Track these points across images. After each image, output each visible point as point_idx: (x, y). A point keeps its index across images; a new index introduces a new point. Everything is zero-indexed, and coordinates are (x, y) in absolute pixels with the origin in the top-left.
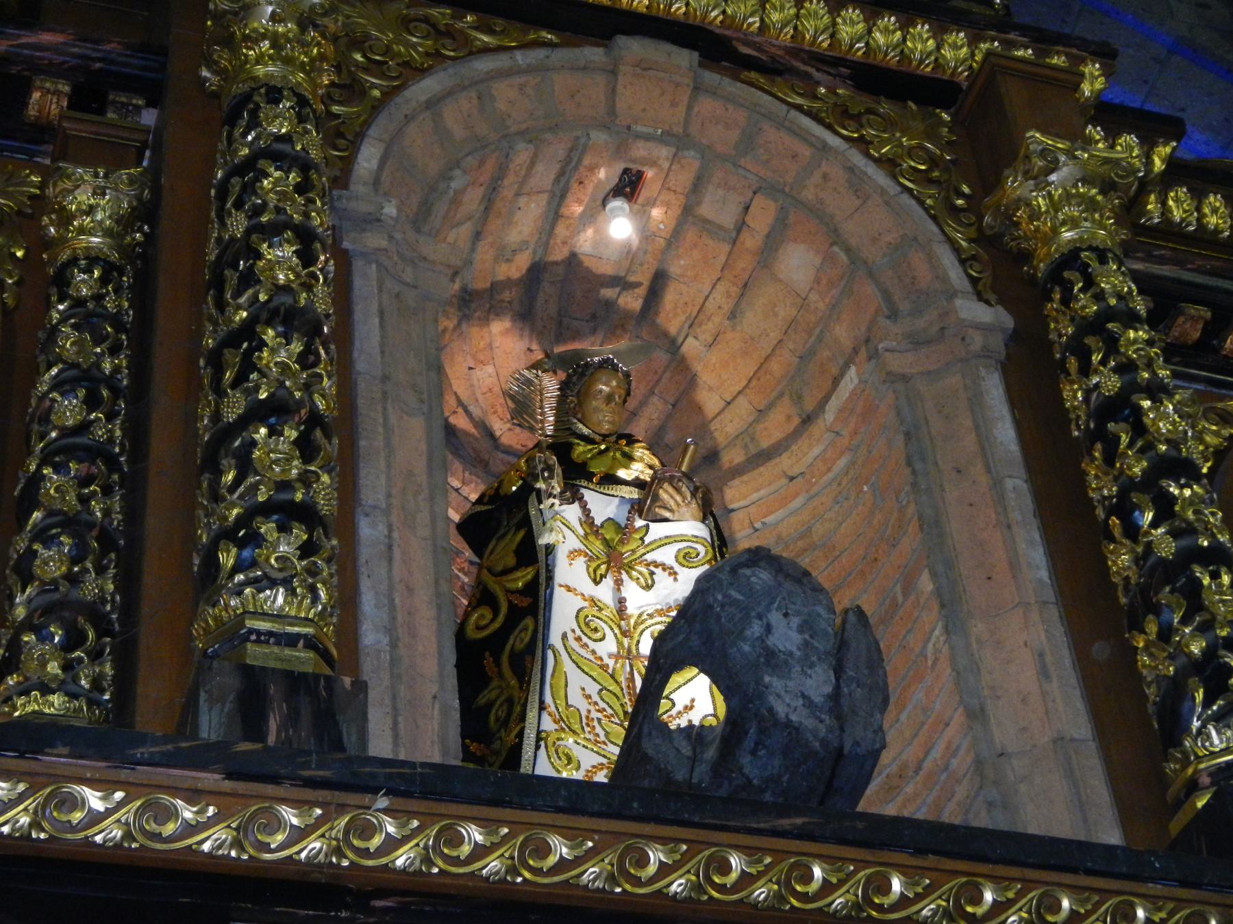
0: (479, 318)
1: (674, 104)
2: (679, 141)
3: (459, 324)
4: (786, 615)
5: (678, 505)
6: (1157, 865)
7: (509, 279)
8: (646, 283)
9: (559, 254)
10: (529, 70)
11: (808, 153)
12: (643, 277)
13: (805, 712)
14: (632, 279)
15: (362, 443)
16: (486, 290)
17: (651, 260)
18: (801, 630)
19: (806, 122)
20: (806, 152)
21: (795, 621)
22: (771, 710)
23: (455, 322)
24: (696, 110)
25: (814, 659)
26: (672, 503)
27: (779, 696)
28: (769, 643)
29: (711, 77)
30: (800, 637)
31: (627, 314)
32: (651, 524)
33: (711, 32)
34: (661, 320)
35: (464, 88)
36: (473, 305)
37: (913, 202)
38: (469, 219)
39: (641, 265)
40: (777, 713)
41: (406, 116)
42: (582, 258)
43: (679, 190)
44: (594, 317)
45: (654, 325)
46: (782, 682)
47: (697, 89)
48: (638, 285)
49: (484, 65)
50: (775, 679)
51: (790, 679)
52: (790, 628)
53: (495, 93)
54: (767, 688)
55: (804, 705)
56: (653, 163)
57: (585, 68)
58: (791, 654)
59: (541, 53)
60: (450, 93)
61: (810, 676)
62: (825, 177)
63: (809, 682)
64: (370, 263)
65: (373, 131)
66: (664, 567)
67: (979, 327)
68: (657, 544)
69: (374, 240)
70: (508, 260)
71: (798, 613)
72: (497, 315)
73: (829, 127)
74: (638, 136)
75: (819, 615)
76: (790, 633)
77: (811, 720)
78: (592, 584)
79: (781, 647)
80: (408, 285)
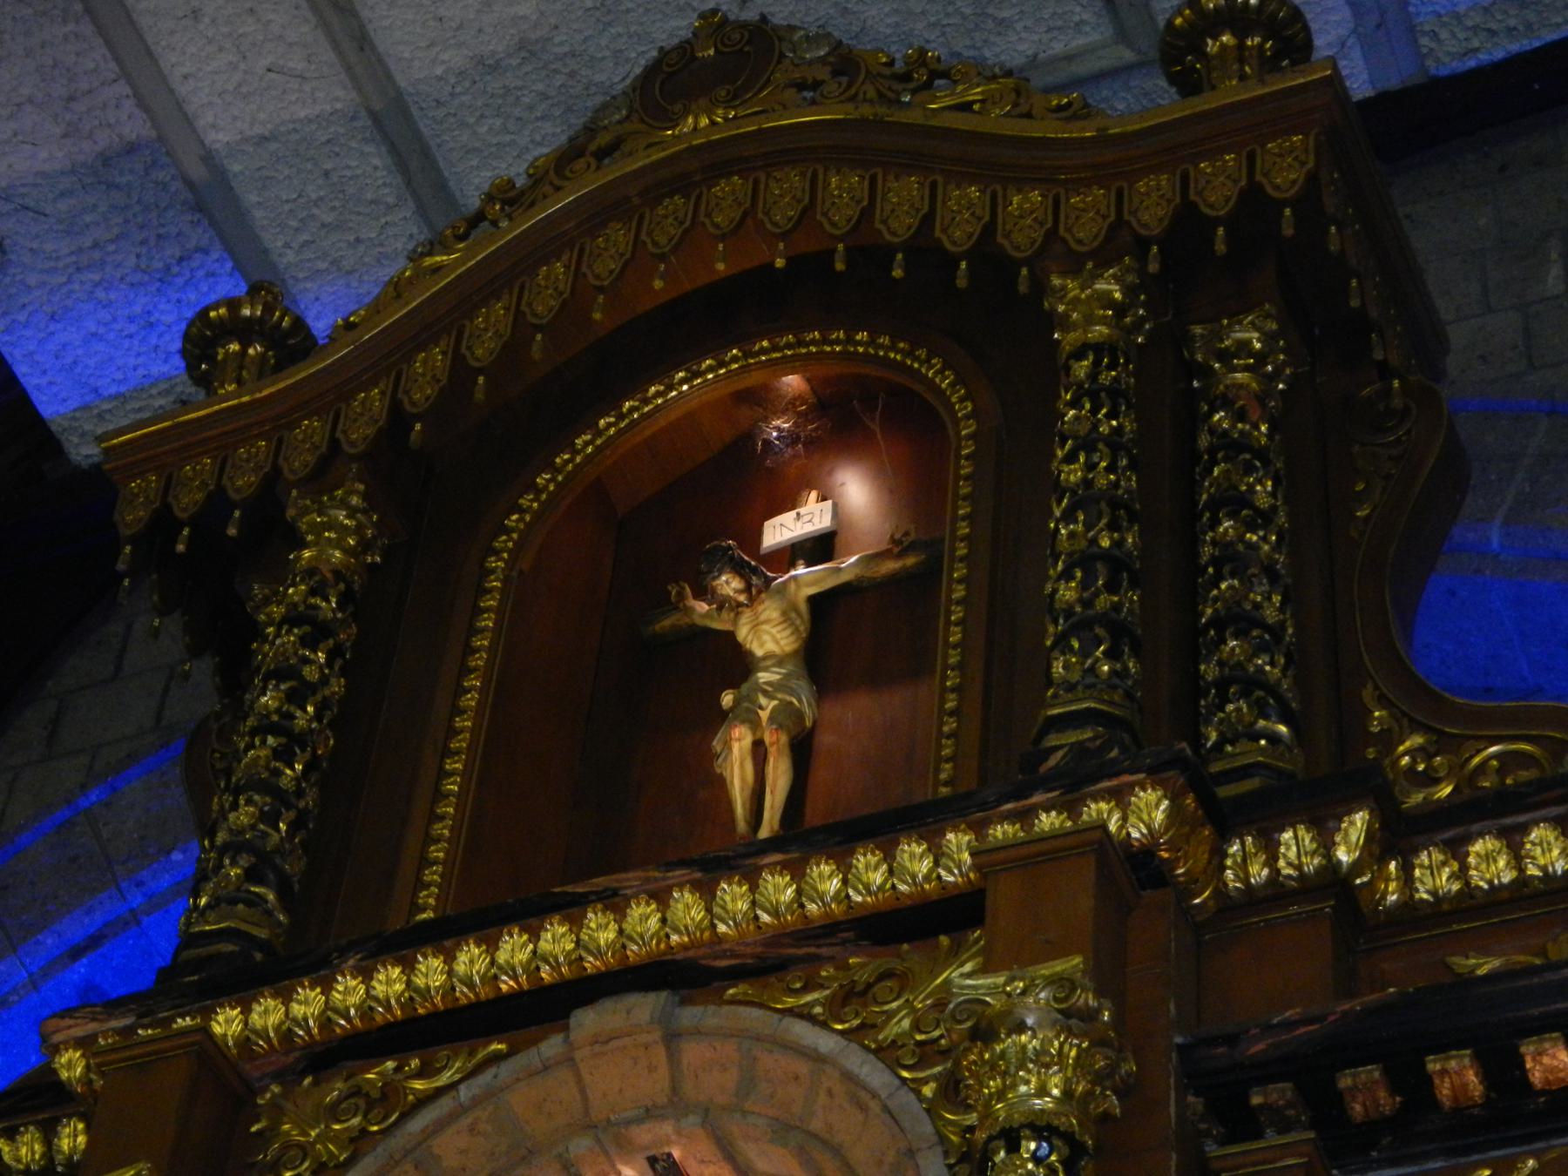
1: (652, 1069)
2: (675, 1105)
10: (476, 1102)
11: (805, 1071)
19: (803, 1032)
20: (803, 1068)
24: (685, 1062)
29: (689, 1015)
33: (674, 962)
35: (397, 1163)
37: (912, 1096)
43: (714, 1160)
47: (672, 1038)
49: (417, 1124)
53: (436, 1151)
56: (669, 1142)
57: (546, 1068)
59: (486, 1078)
62: (830, 1093)
73: (824, 1025)
74: (629, 1123)
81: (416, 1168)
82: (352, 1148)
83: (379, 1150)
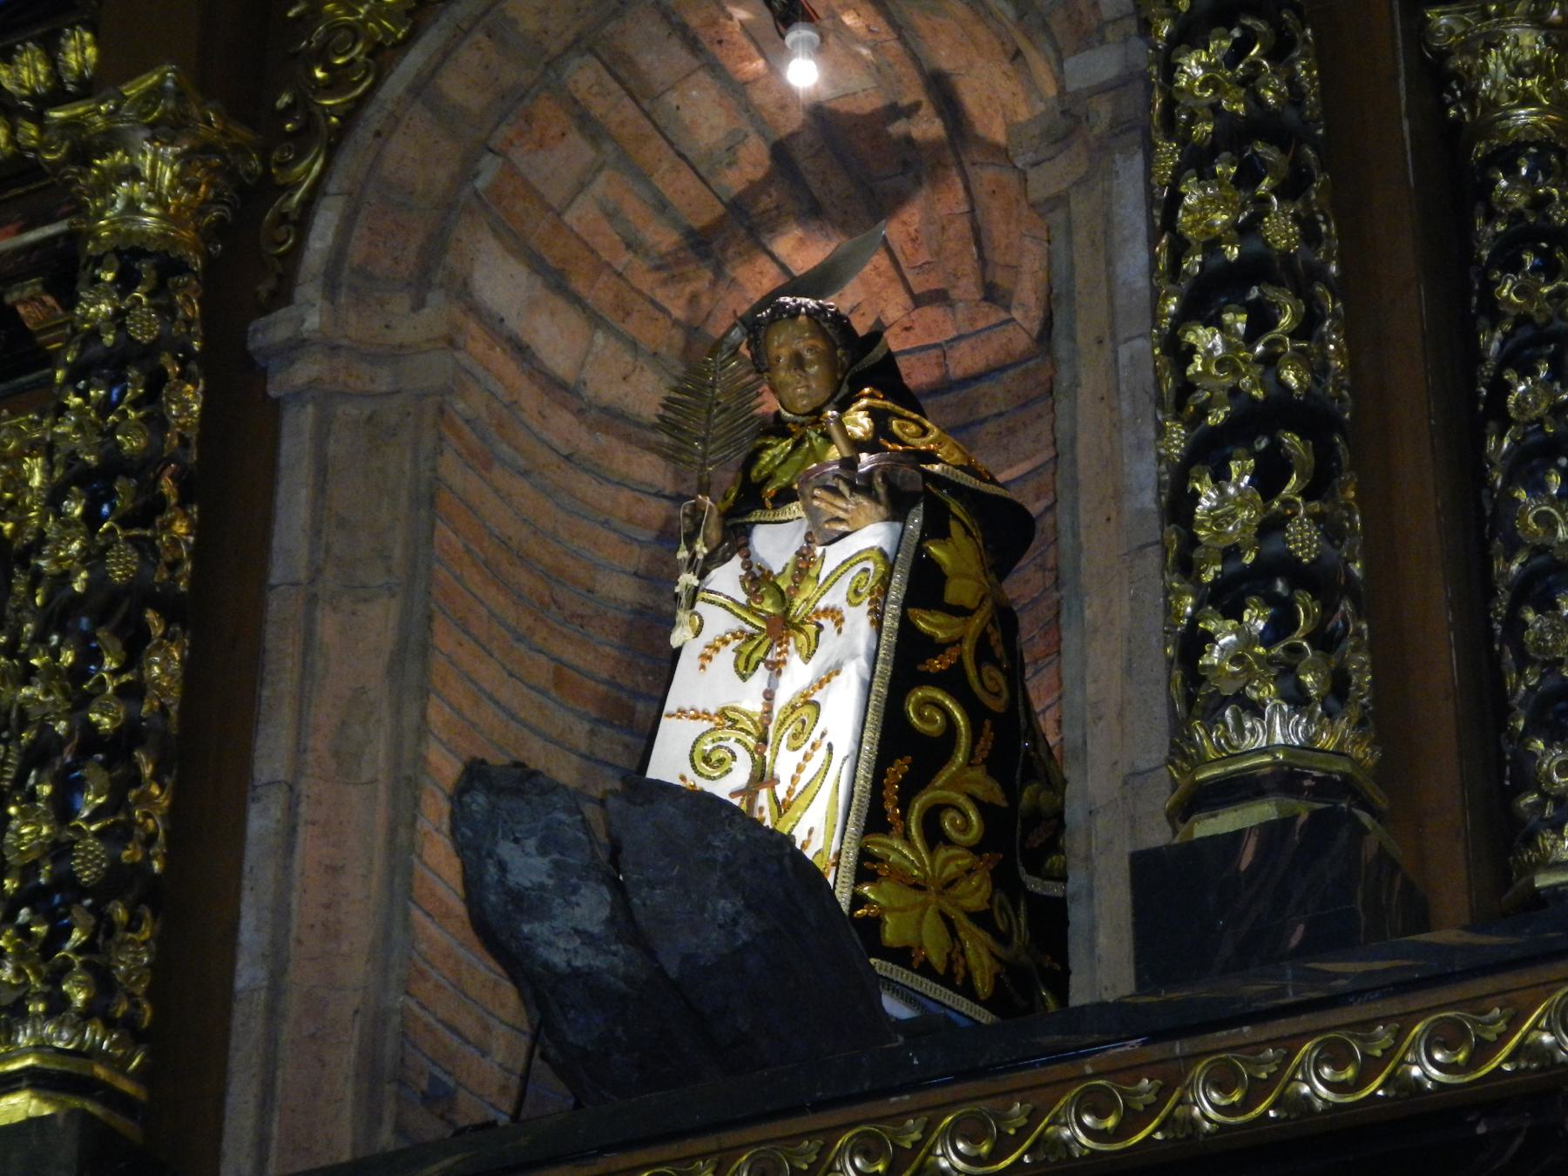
0: (740, 254)
3: (718, 271)
4: (516, 841)
5: (846, 511)
6: (916, 1062)
7: (752, 184)
8: (924, 99)
9: (793, 121)
12: (913, 93)
13: (589, 952)
14: (905, 101)
15: (266, 693)
16: (723, 217)
17: (904, 70)
18: (543, 850)
21: (531, 844)
22: (546, 965)
23: (709, 275)
25: (574, 880)
26: (841, 514)
27: (550, 944)
28: (511, 884)
30: (547, 859)
31: (935, 146)
32: (827, 548)
34: (980, 130)
35: (467, 33)
36: (715, 245)
38: (600, 169)
39: (900, 81)
40: (555, 965)
41: (378, 134)
42: (833, 105)
44: (905, 164)
45: (981, 142)
46: (547, 924)
48: (916, 106)
50: (537, 924)
51: (553, 917)
52: (528, 855)
54: (530, 939)
55: (583, 943)
58: (542, 886)
60: (446, 53)
61: (578, 904)
63: (578, 911)
64: (303, 406)
65: (332, 187)
66: (831, 612)
67: (1102, 89)
68: (832, 579)
69: (304, 371)
70: (729, 165)
71: (531, 833)
72: (772, 230)
75: (561, 822)
76: (532, 861)
77: (602, 958)
78: (739, 681)
79: (528, 884)
80: (387, 394)
81: (489, 36)
82: (411, 21)
83: (443, 20)
